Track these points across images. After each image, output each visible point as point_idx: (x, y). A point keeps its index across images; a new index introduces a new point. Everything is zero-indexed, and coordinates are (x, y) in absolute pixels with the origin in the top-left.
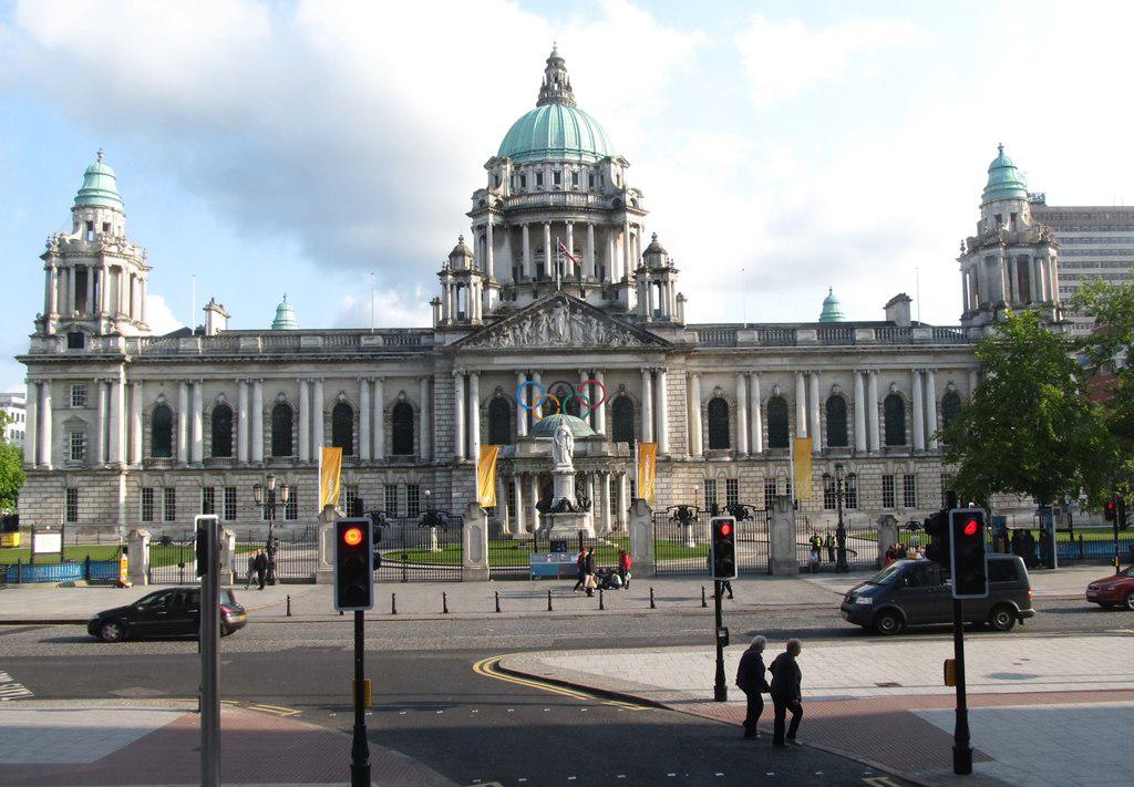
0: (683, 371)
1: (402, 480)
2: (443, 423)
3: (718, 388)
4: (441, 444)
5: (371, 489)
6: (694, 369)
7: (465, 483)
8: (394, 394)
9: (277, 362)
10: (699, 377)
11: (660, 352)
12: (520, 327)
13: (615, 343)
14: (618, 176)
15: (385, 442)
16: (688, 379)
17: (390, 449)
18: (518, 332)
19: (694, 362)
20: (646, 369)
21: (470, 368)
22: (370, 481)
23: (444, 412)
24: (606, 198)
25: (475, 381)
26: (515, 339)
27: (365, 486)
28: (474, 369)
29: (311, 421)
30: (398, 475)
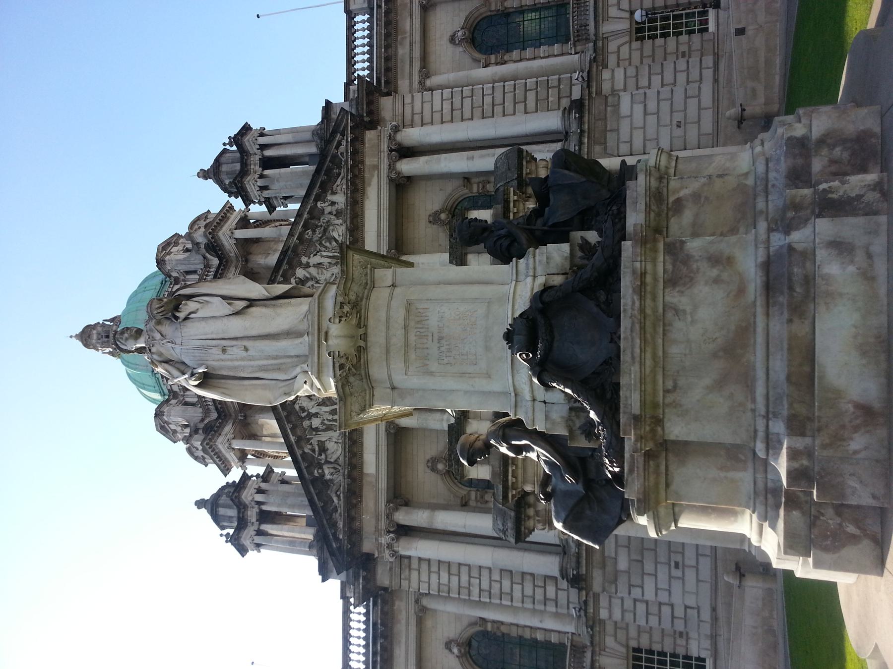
0: (408, 100)
2: (496, 586)
3: (452, 40)
4: (539, 592)
6: (416, 85)
7: (623, 565)
10: (428, 76)
11: (357, 140)
12: (310, 416)
13: (339, 232)
14: (187, 250)
16: (431, 90)
18: (316, 422)
19: (403, 84)
20: (391, 167)
21: (383, 524)
23: (475, 582)
24: (207, 266)
26: (329, 428)
28: (384, 517)
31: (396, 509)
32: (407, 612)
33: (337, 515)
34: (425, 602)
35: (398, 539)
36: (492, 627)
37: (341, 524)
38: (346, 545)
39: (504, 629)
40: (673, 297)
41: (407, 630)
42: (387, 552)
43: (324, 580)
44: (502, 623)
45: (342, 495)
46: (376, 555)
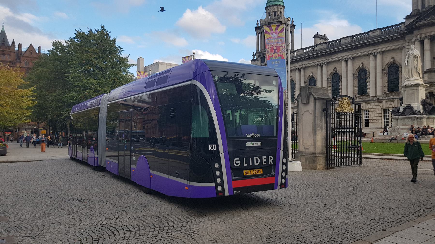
1: (391, 106)
5: (374, 111)
8: (388, 59)
9: (331, 54)
15: (383, 87)
17: (386, 89)
21: (424, 36)
22: (374, 107)
25: (427, 42)
27: (372, 110)
29: (347, 80)
30: (389, 103)
31: (429, 39)
32: (399, 45)
33: (424, 21)
34: (404, 49)
35: (420, 41)
36: (400, 70)
37: (421, 23)
38: (414, 27)
39: (400, 73)
40: (410, 120)
41: (395, 46)
42: (414, 39)
43: (404, 18)
44: (402, 73)
45: (430, 21)
46: (413, 36)
